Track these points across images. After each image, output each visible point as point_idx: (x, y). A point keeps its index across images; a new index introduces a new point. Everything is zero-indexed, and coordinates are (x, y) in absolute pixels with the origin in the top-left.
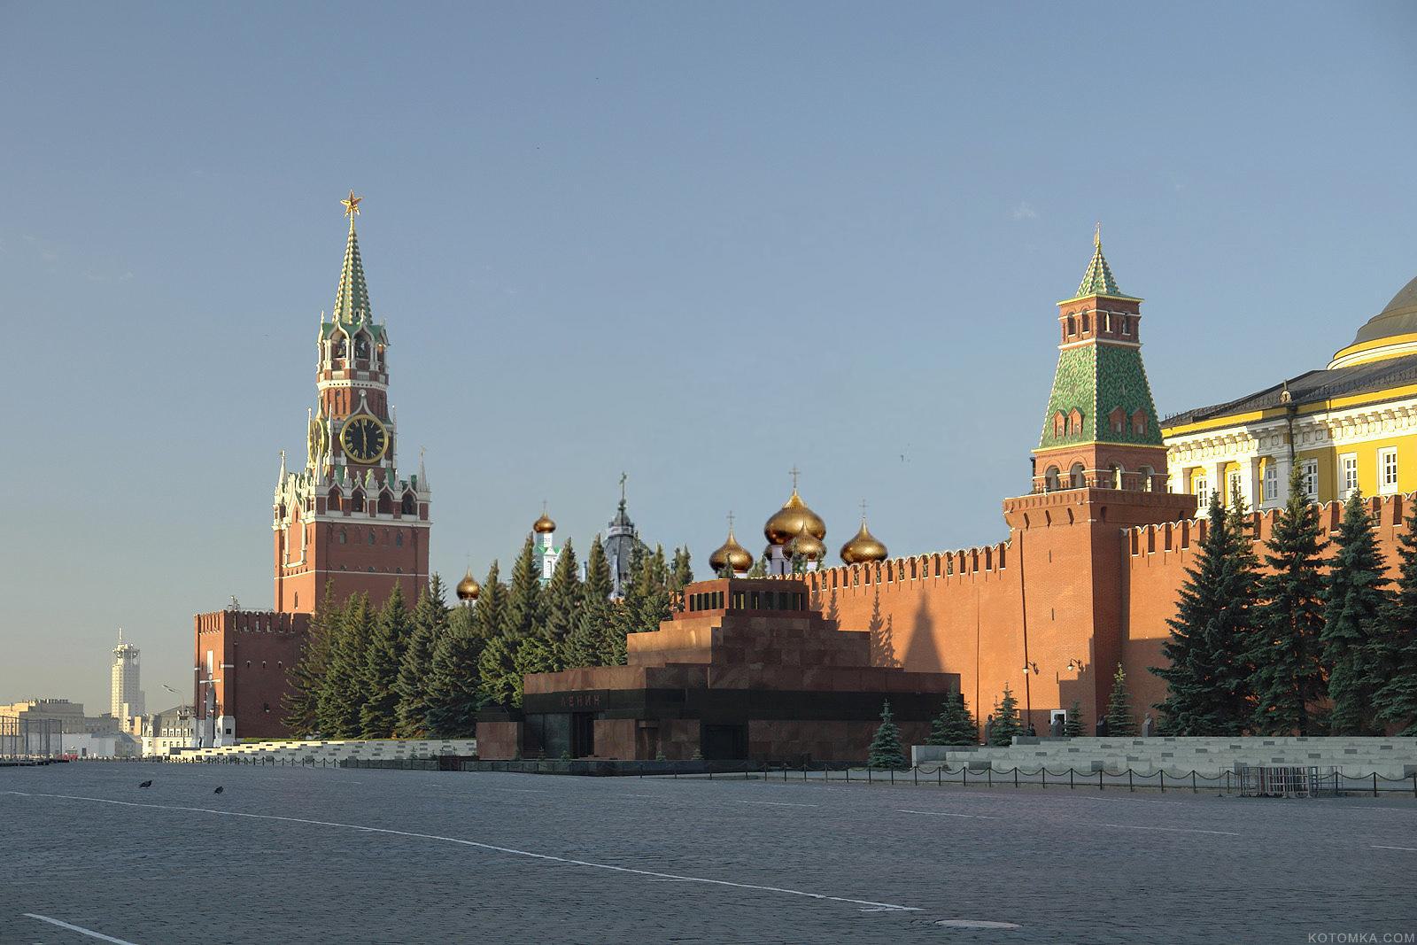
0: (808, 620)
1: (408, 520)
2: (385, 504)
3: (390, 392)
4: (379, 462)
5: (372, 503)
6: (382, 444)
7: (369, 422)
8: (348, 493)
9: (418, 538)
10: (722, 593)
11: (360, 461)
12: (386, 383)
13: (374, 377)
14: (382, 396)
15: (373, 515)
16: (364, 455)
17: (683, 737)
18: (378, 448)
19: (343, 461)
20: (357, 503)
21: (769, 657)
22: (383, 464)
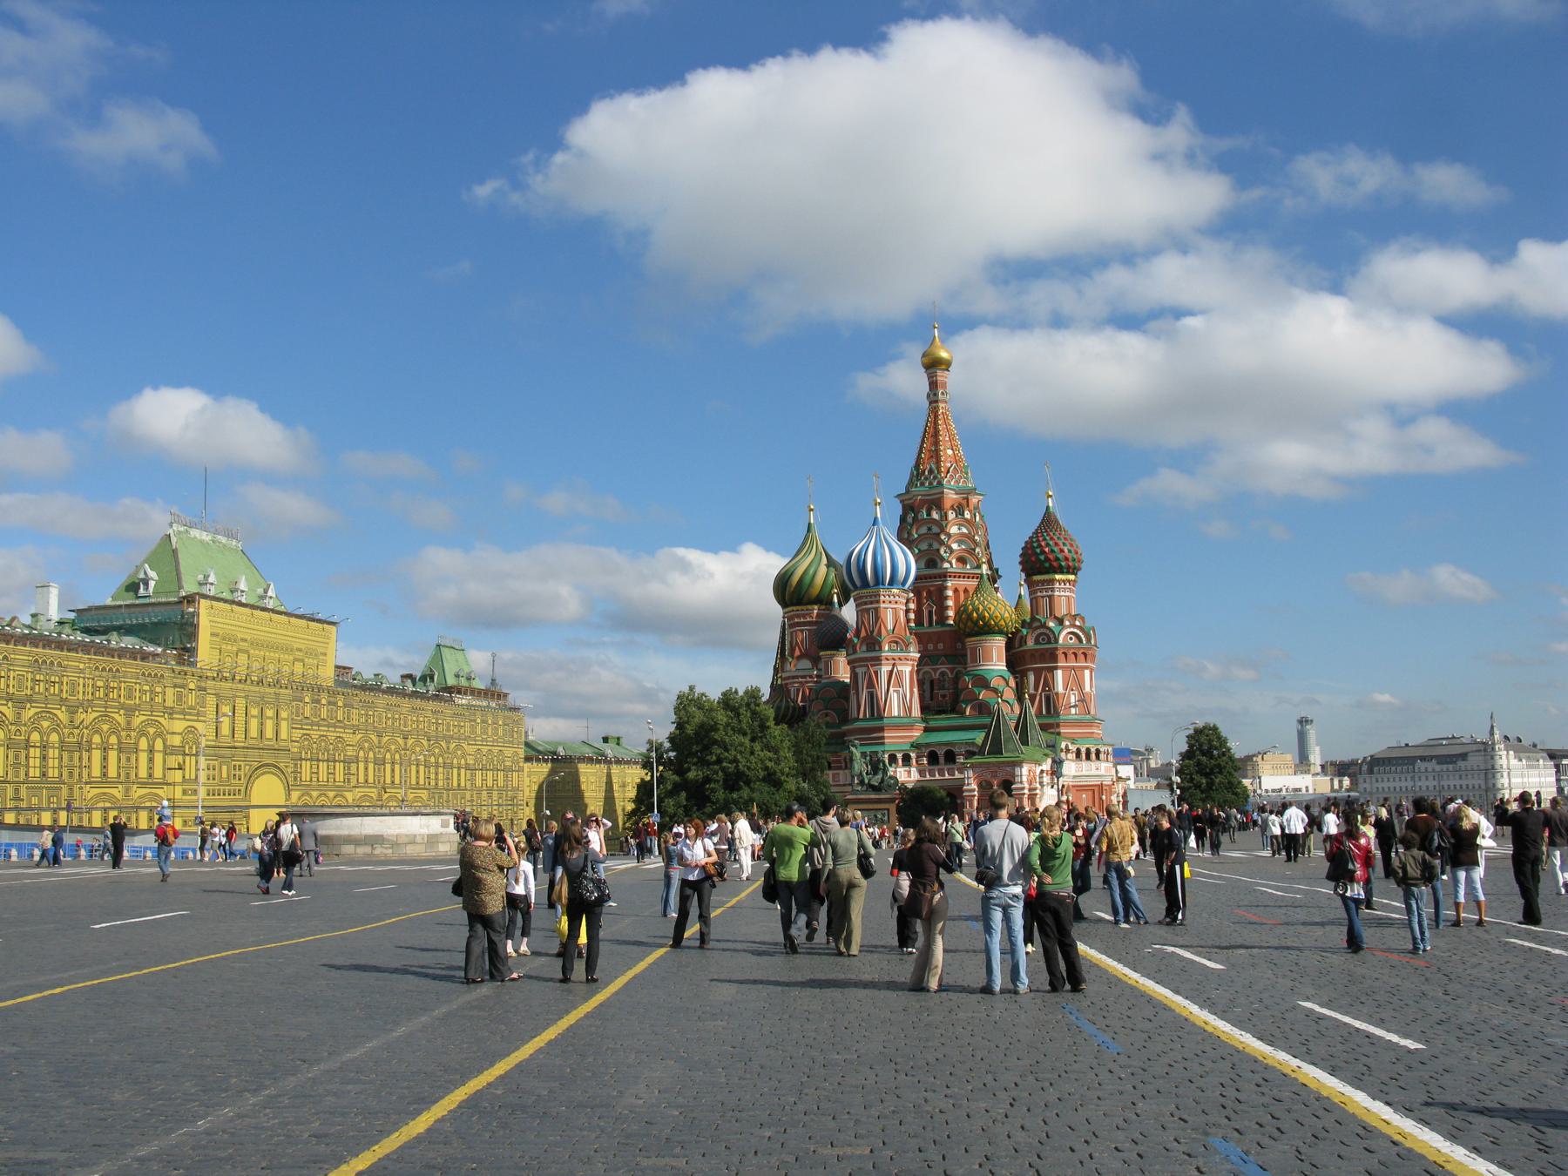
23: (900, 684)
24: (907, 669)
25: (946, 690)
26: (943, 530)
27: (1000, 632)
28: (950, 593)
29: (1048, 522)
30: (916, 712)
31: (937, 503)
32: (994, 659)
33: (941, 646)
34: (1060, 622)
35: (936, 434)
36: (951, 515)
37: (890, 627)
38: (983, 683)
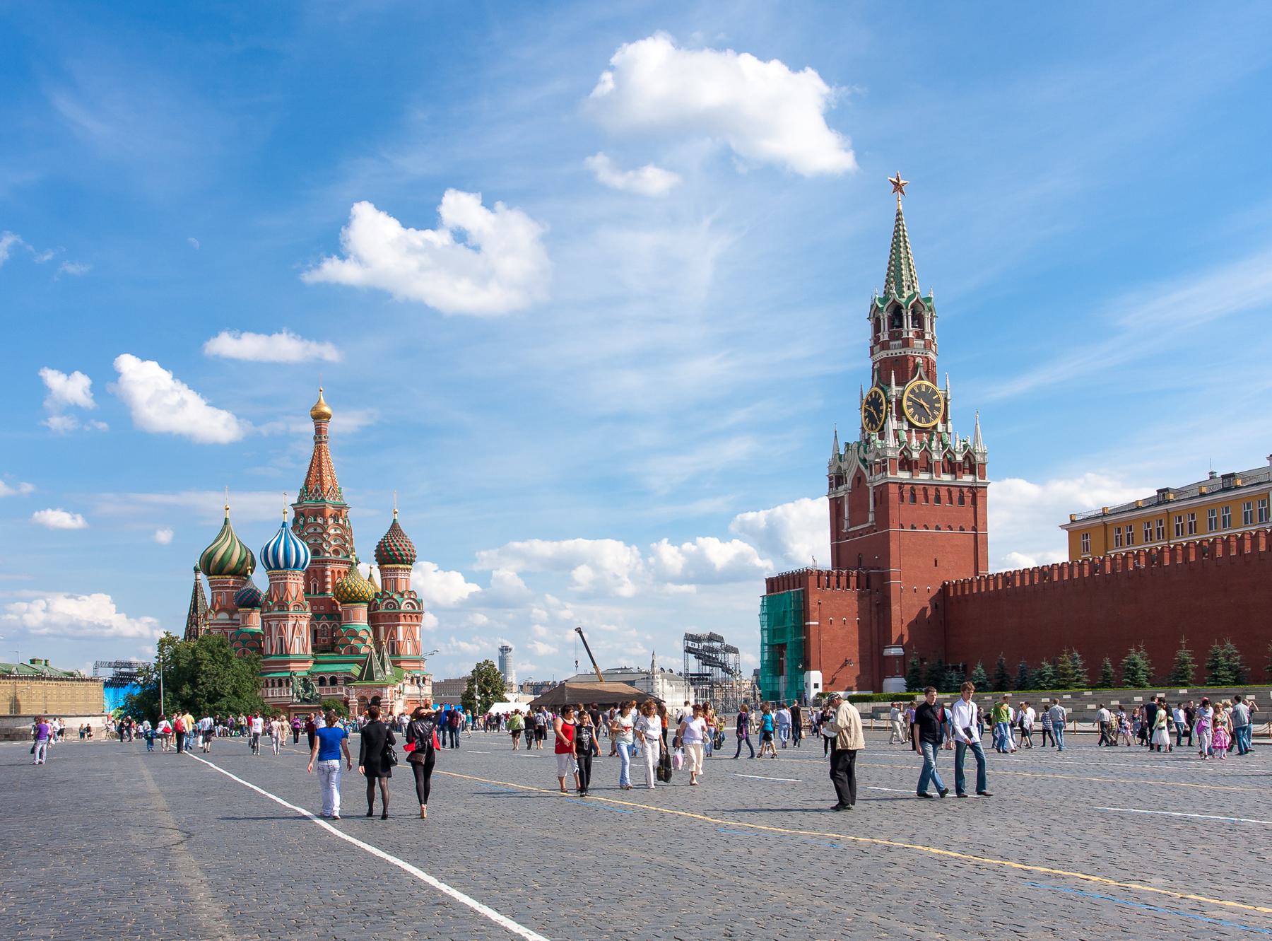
1: (967, 479)
4: (935, 427)
9: (976, 495)
22: (940, 428)
23: (300, 632)
24: (304, 623)
25: (328, 640)
26: (325, 531)
27: (365, 601)
28: (329, 573)
29: (395, 528)
30: (310, 652)
31: (320, 513)
32: (360, 620)
33: (322, 608)
34: (402, 595)
35: (320, 465)
36: (331, 521)
37: (294, 595)
38: (354, 634)
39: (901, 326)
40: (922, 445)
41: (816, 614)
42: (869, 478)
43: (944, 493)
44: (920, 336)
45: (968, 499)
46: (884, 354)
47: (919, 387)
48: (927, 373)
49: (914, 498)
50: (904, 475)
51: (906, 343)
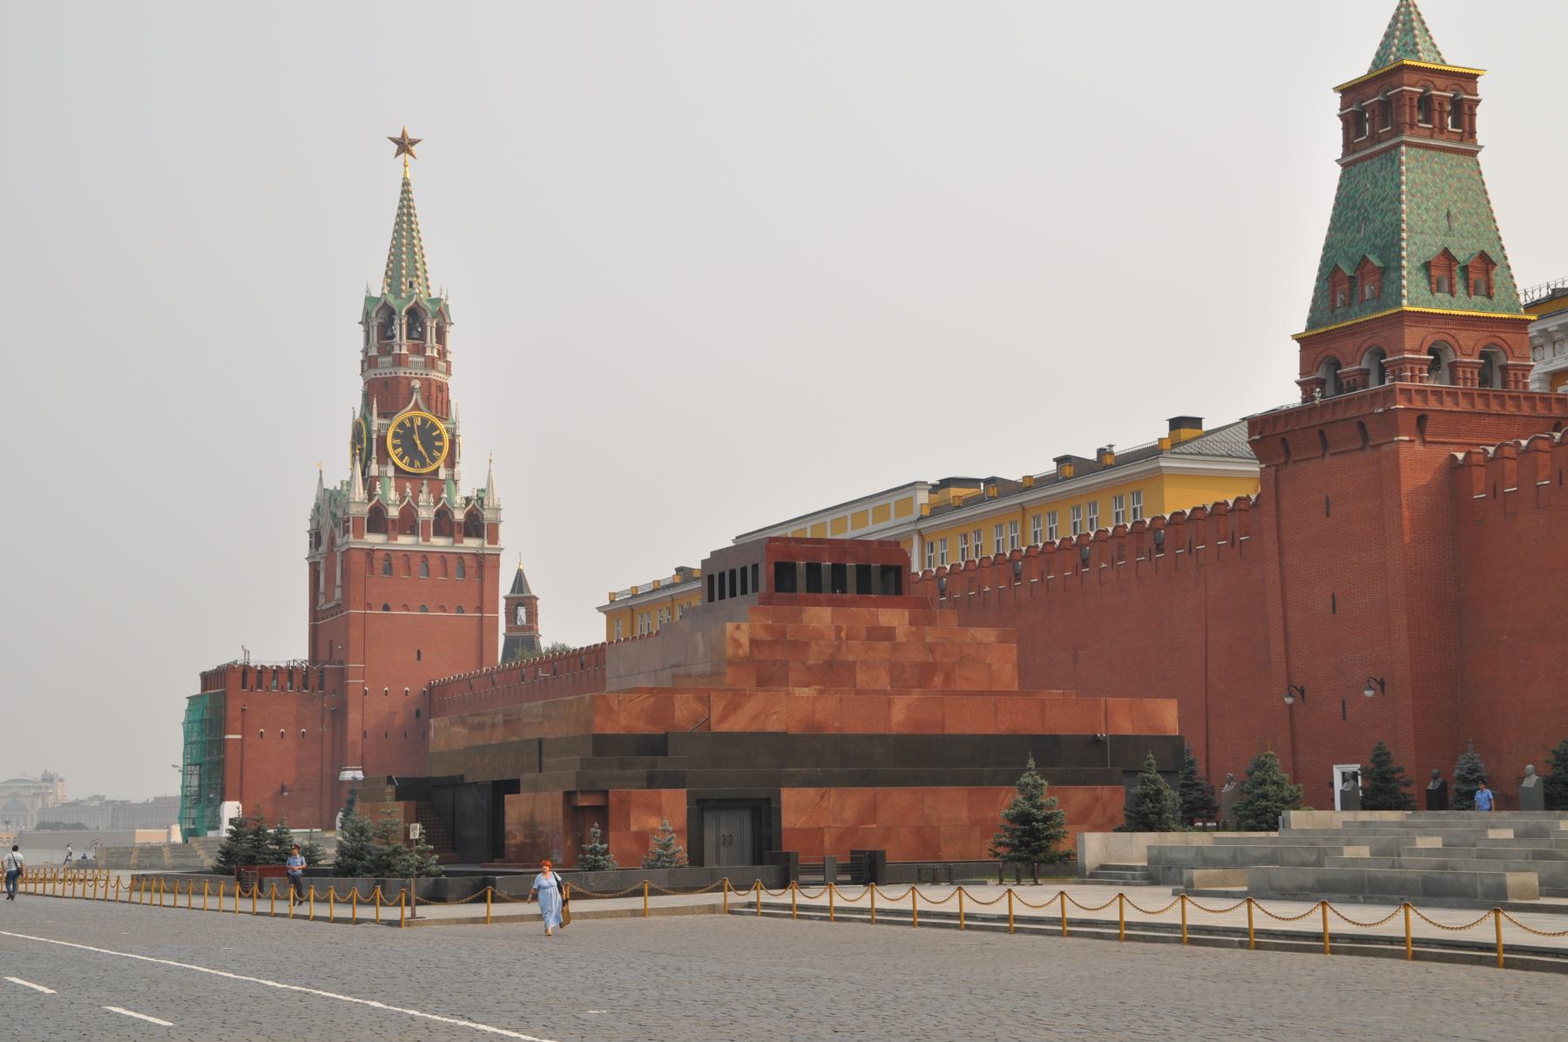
0: (906, 612)
1: (471, 544)
2: (443, 524)
3: (452, 383)
4: (436, 472)
5: (426, 522)
6: (440, 449)
7: (424, 420)
8: (393, 512)
10: (755, 567)
11: (411, 470)
12: (448, 372)
13: (431, 363)
14: (442, 388)
15: (426, 539)
16: (417, 463)
17: (653, 822)
18: (436, 453)
19: (391, 471)
20: (408, 523)
21: (833, 673)
22: (443, 474)
39: (393, 336)
40: (402, 498)
41: (238, 724)
42: (338, 541)
43: (434, 562)
44: (420, 350)
45: (471, 572)
46: (372, 374)
47: (411, 420)
48: (427, 399)
49: (389, 570)
50: (376, 540)
51: (399, 361)
